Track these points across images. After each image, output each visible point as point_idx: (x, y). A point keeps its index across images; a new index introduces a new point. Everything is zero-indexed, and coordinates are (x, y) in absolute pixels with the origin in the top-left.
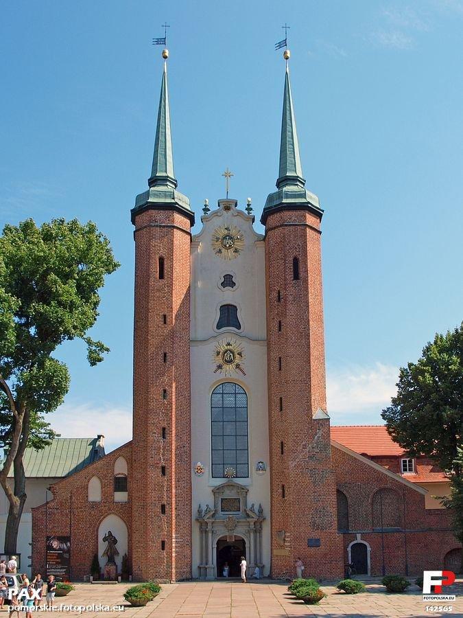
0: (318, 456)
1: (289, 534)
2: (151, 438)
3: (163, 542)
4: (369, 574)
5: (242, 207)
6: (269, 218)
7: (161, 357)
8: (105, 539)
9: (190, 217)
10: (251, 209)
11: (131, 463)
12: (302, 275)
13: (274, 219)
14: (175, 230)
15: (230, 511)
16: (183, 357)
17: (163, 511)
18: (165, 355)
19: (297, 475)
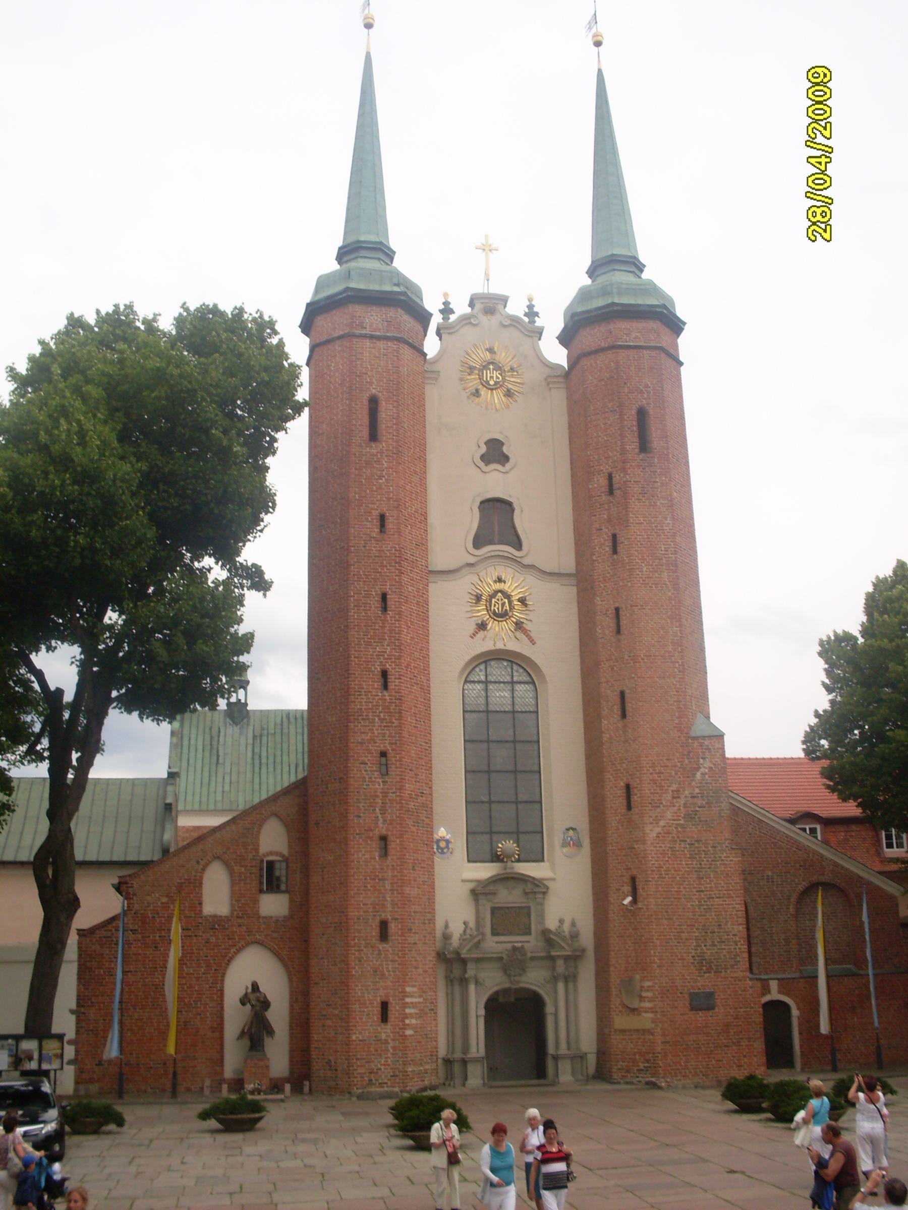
1: (648, 984)
3: (385, 1006)
5: (515, 308)
7: (375, 603)
10: (537, 314)
12: (656, 443)
15: (511, 934)
16: (418, 603)
18: (384, 597)
19: (664, 854)
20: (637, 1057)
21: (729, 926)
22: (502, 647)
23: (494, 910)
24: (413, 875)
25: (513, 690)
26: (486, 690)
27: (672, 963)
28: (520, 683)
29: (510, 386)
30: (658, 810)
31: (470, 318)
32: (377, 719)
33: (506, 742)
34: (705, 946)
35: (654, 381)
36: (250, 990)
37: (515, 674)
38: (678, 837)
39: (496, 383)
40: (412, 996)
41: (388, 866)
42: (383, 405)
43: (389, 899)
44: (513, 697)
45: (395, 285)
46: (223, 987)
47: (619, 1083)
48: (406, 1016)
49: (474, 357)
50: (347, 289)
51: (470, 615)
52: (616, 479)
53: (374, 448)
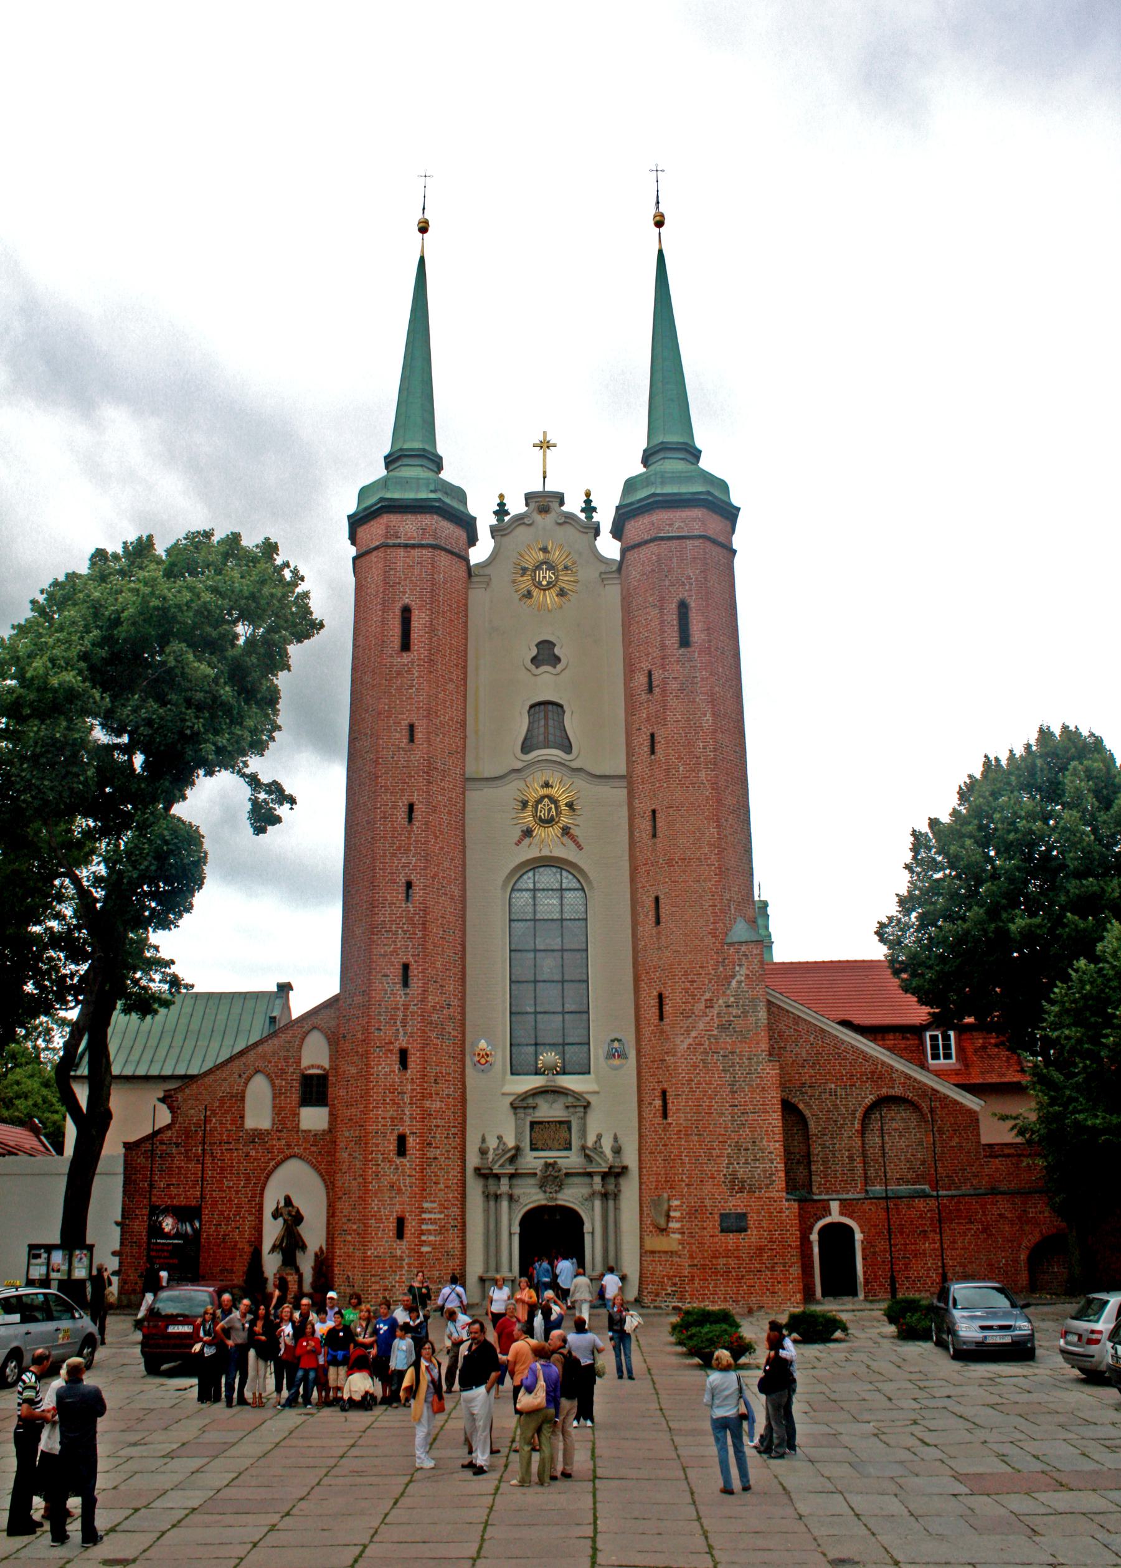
0: (739, 1024)
1: (677, 1203)
2: (377, 985)
3: (401, 1222)
4: (861, 1296)
7: (401, 814)
8: (276, 1215)
9: (468, 525)
10: (594, 509)
11: (334, 1040)
13: (636, 529)
15: (550, 1149)
16: (450, 813)
17: (402, 1150)
18: (411, 807)
19: (695, 1066)
20: (666, 1280)
21: (765, 1143)
22: (549, 854)
23: (532, 1124)
24: (434, 1089)
25: (562, 897)
26: (534, 898)
27: (701, 1181)
28: (569, 890)
29: (563, 585)
30: (690, 1020)
31: (522, 519)
32: (400, 932)
33: (553, 951)
34: (738, 1164)
35: (698, 571)
36: (282, 1204)
37: (564, 881)
38: (710, 1049)
39: (549, 583)
40: (430, 1212)
41: (407, 1079)
42: (415, 614)
43: (408, 1113)
44: (562, 905)
45: (432, 491)
46: (262, 1201)
47: (648, 1307)
48: (422, 1233)
49: (527, 558)
50: (382, 499)
51: (515, 821)
52: (656, 676)
53: (406, 658)
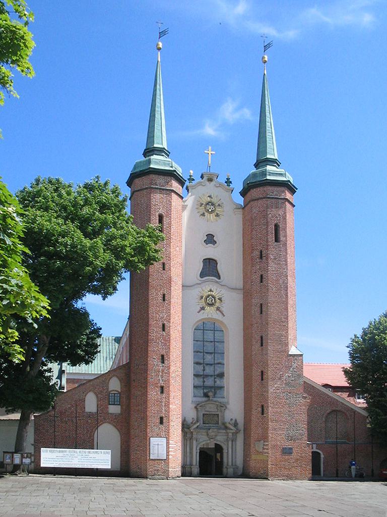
6: (252, 191)
10: (231, 182)
14: (173, 193)
17: (161, 422)
51: (198, 304)
